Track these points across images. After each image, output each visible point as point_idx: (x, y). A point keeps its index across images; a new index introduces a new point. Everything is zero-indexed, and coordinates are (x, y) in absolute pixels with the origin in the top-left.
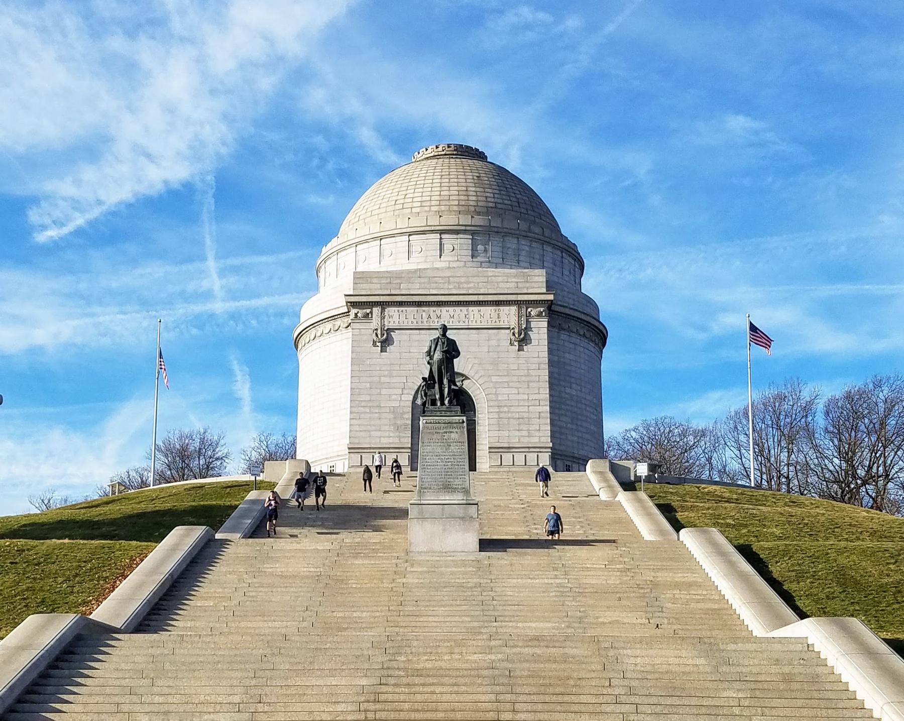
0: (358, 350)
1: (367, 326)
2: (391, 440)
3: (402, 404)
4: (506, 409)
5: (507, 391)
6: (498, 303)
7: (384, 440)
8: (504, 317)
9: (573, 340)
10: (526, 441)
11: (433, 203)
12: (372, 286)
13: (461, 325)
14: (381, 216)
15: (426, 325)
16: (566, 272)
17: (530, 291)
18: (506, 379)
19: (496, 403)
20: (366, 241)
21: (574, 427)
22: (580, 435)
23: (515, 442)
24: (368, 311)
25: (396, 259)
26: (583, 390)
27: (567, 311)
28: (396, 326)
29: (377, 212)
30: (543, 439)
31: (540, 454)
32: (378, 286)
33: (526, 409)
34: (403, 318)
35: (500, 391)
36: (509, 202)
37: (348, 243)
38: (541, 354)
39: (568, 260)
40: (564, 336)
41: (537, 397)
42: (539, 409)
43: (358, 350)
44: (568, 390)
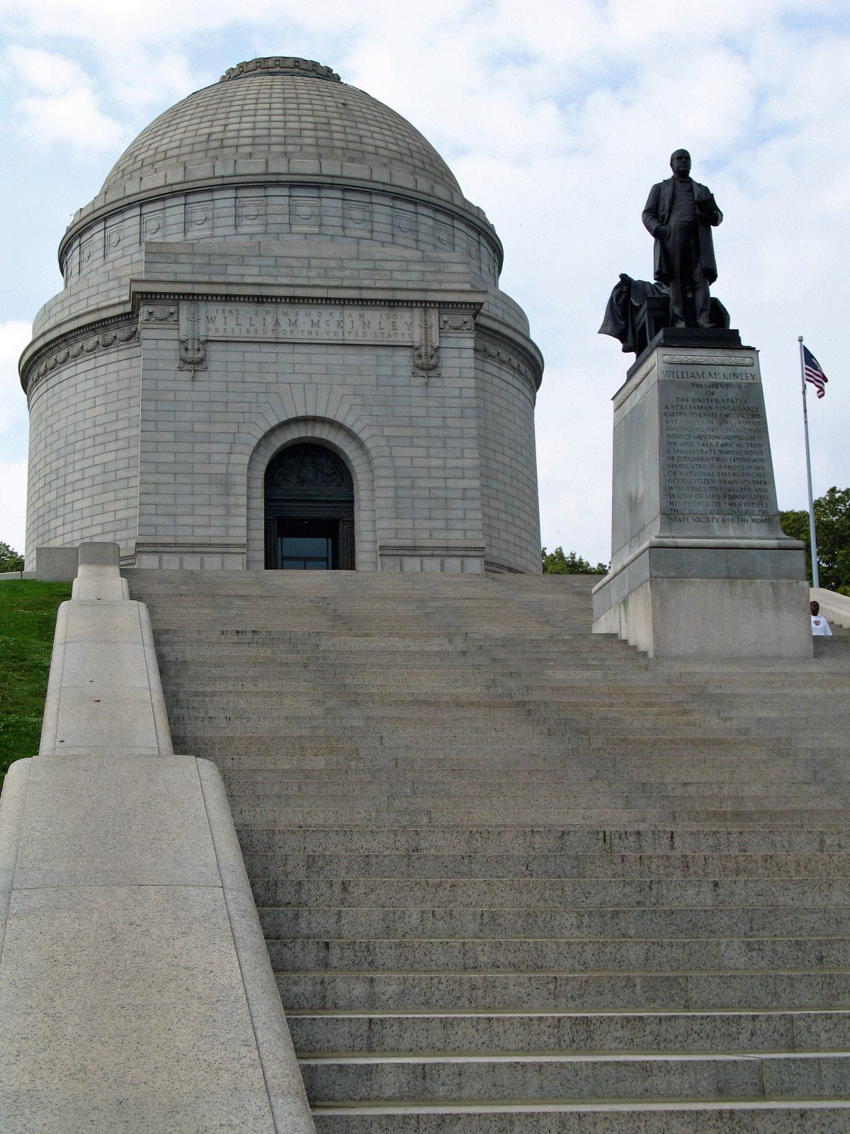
0: (153, 375)
1: (174, 335)
2: (212, 531)
3: (231, 469)
4: (407, 483)
5: (407, 452)
6: (392, 304)
7: (200, 532)
8: (402, 327)
9: (505, 376)
10: (439, 539)
11: (274, 140)
12: (177, 268)
13: (332, 338)
14: (186, 158)
15: (270, 336)
16: (485, 268)
17: (444, 286)
18: (408, 432)
19: (391, 472)
20: (161, 198)
21: (509, 518)
22: (517, 531)
23: (424, 539)
24: (172, 309)
25: (213, 228)
26: (520, 459)
27: (495, 326)
28: (219, 335)
29: (175, 152)
30: (470, 535)
31: (466, 560)
32: (188, 268)
33: (441, 483)
34: (231, 322)
35: (396, 451)
36: (395, 148)
37: (126, 201)
38: (466, 393)
39: (486, 251)
40: (491, 368)
41: (460, 463)
42: (462, 484)
43: (153, 375)
44: (499, 457)
